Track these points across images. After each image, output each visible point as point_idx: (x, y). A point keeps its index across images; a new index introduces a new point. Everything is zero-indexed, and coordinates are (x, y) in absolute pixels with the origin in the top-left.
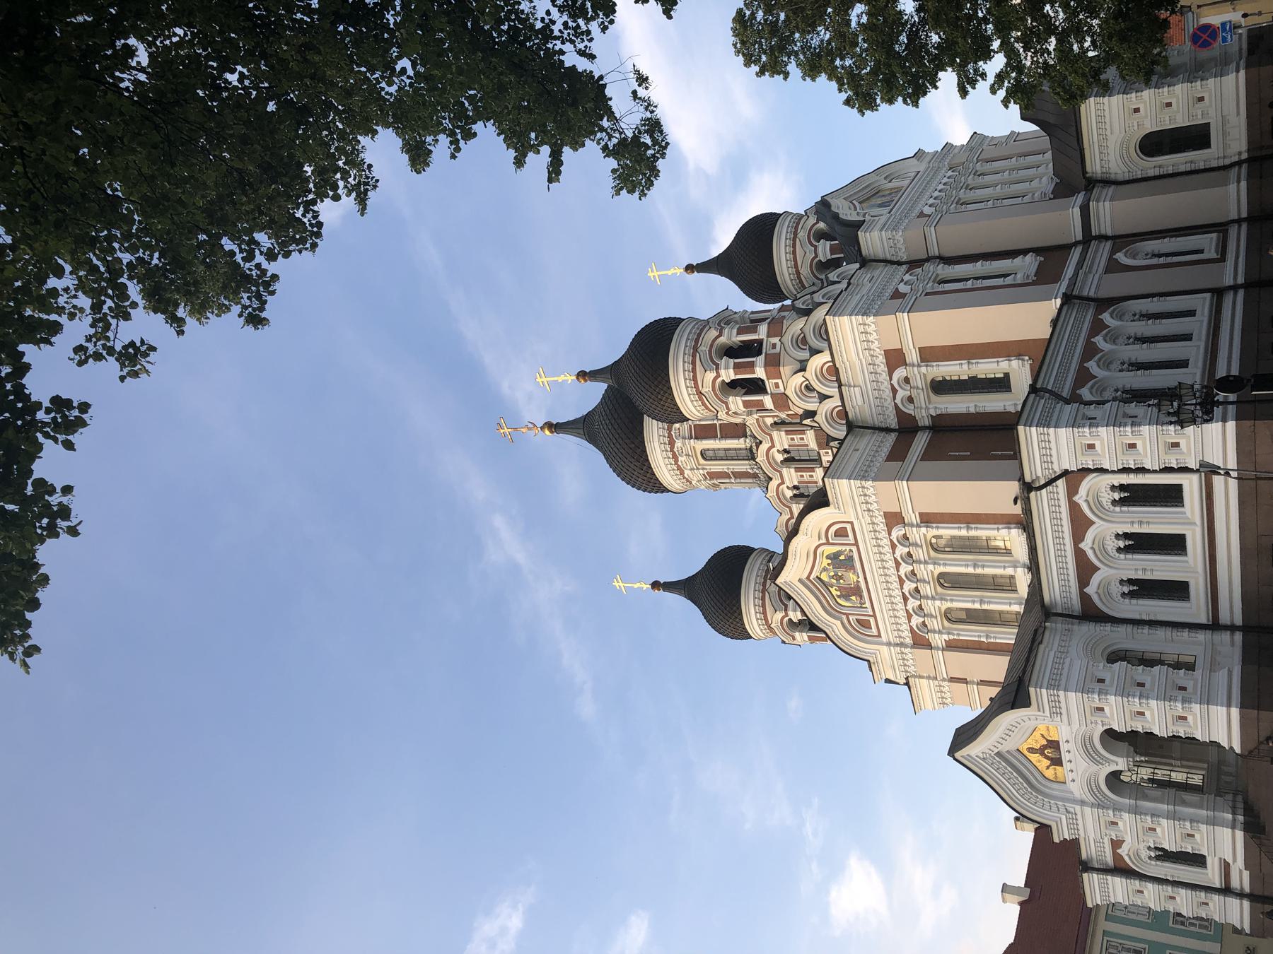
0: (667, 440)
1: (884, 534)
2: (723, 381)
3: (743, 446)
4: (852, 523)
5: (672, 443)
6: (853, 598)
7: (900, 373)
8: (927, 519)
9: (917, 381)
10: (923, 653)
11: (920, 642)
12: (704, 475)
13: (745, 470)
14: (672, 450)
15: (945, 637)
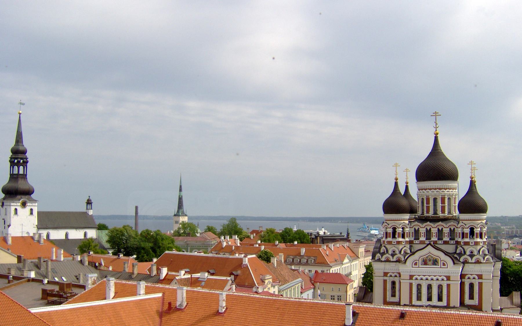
0: (441, 188)
1: (444, 275)
2: (474, 229)
3: (438, 213)
4: (447, 268)
5: (440, 189)
6: (424, 263)
7: (477, 277)
8: (448, 286)
9: (473, 281)
10: (408, 278)
11: (411, 277)
12: (429, 196)
13: (430, 211)
14: (438, 189)
15: (413, 284)
